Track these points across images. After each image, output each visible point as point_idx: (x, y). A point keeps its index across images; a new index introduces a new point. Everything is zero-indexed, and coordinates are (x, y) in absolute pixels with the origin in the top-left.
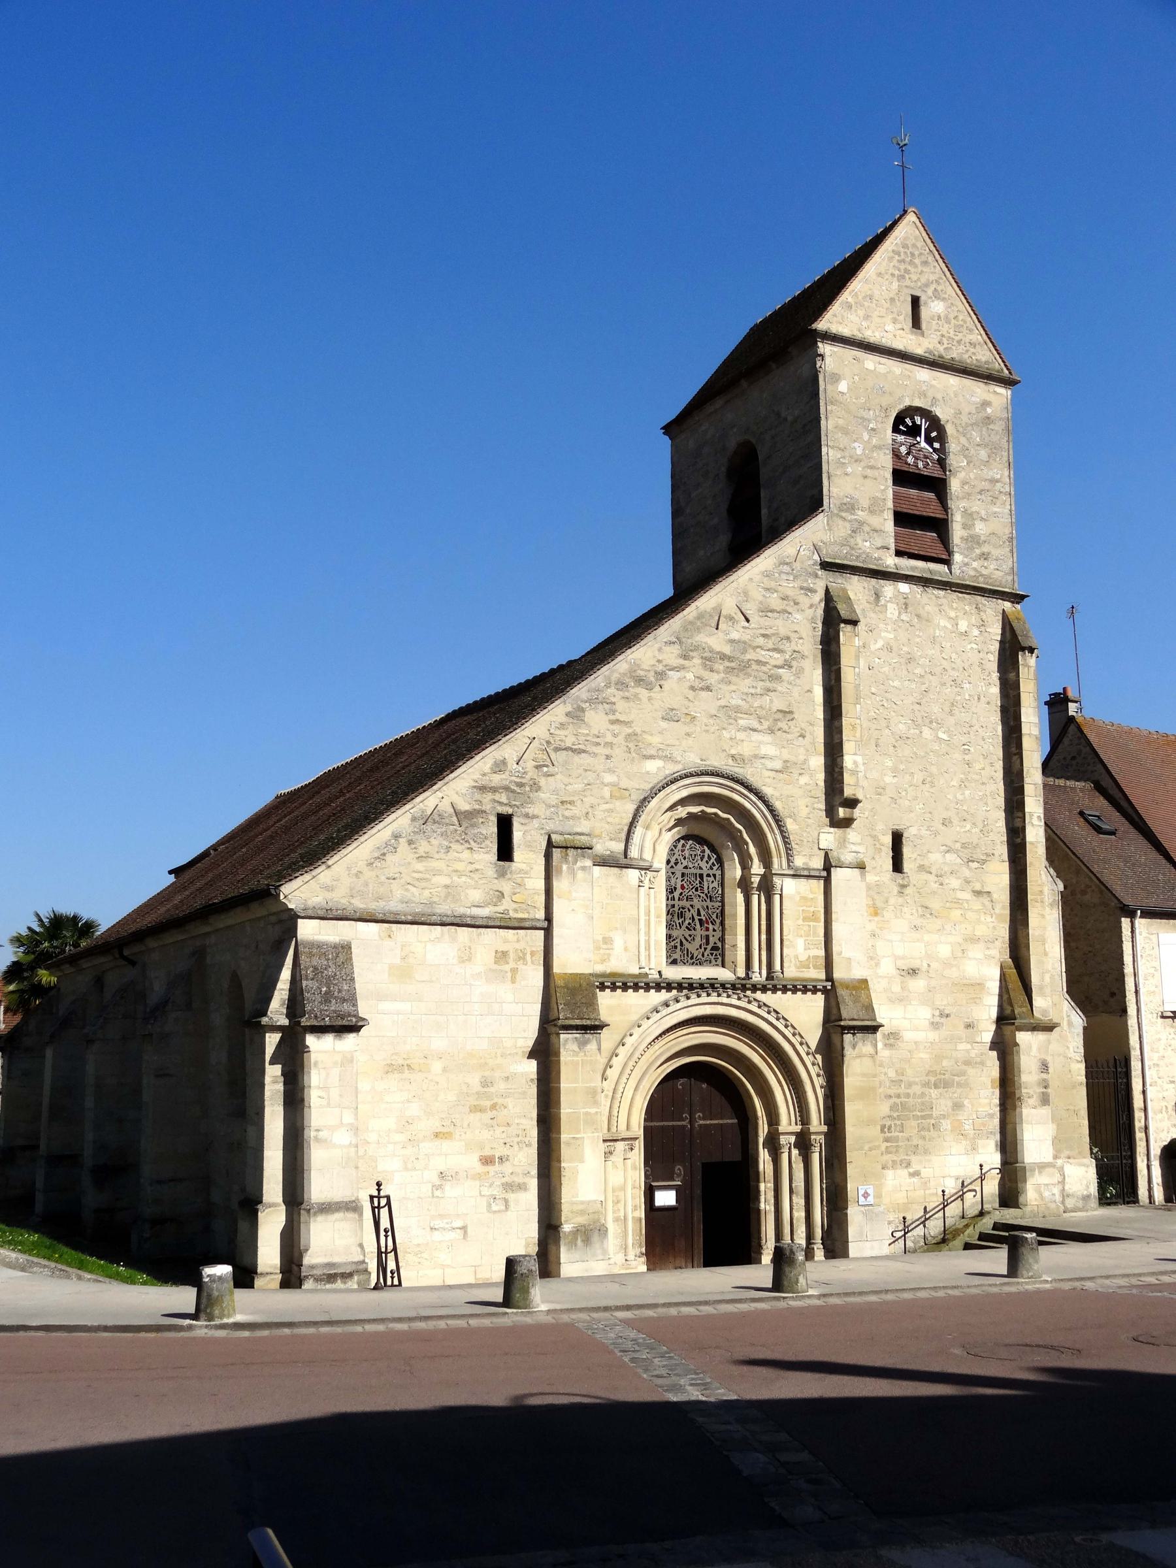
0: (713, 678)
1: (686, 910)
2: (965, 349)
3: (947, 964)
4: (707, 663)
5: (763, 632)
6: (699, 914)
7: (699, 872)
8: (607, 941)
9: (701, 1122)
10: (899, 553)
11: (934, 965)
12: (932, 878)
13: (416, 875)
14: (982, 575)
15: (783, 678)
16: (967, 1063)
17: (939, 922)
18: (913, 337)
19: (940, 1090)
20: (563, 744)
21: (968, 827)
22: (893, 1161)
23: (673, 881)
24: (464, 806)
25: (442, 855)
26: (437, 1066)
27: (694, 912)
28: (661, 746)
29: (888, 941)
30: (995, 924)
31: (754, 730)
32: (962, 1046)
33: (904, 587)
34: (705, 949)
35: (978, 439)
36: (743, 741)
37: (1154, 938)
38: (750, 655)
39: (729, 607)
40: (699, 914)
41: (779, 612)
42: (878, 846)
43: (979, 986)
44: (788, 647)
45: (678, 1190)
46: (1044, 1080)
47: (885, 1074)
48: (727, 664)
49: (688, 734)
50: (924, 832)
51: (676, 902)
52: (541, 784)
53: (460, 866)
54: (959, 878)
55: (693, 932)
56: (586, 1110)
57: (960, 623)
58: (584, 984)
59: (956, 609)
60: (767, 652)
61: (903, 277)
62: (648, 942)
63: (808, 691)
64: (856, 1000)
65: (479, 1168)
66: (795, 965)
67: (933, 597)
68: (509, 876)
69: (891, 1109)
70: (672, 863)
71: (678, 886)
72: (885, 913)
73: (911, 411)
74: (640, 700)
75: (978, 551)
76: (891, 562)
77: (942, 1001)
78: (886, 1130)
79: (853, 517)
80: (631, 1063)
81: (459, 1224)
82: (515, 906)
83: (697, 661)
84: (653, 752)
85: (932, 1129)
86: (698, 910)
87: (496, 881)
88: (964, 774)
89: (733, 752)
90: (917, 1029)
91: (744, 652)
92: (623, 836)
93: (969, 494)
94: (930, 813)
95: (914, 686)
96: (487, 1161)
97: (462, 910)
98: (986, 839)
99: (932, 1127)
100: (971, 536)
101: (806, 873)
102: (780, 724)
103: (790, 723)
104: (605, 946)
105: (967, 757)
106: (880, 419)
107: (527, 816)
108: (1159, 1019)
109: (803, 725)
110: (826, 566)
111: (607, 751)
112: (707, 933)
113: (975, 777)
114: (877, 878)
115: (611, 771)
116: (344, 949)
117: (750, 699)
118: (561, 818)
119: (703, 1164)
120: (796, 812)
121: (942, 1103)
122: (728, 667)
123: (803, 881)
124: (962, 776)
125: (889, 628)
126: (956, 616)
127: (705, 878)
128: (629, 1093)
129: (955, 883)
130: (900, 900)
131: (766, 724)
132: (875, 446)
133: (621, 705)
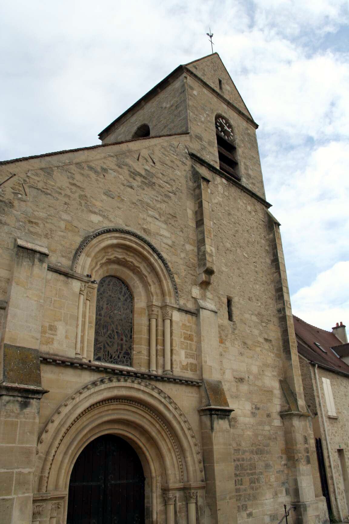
0: (135, 184)
1: (109, 324)
4: (132, 174)
8: (52, 328)
11: (251, 377)
19: (259, 456)
20: (35, 185)
21: (259, 304)
23: (101, 303)
28: (101, 209)
31: (157, 219)
34: (120, 353)
36: (150, 223)
39: (145, 153)
43: (270, 392)
51: (102, 317)
52: (14, 204)
55: (112, 340)
56: (19, 470)
62: (82, 337)
63: (185, 210)
66: (180, 367)
71: (105, 306)
74: (91, 178)
80: (64, 430)
84: (97, 211)
86: (117, 325)
89: (145, 226)
90: (245, 416)
92: (71, 256)
94: (243, 292)
104: (50, 332)
111: (67, 200)
117: (154, 201)
118: (26, 231)
121: (260, 465)
122: (143, 181)
128: (59, 457)
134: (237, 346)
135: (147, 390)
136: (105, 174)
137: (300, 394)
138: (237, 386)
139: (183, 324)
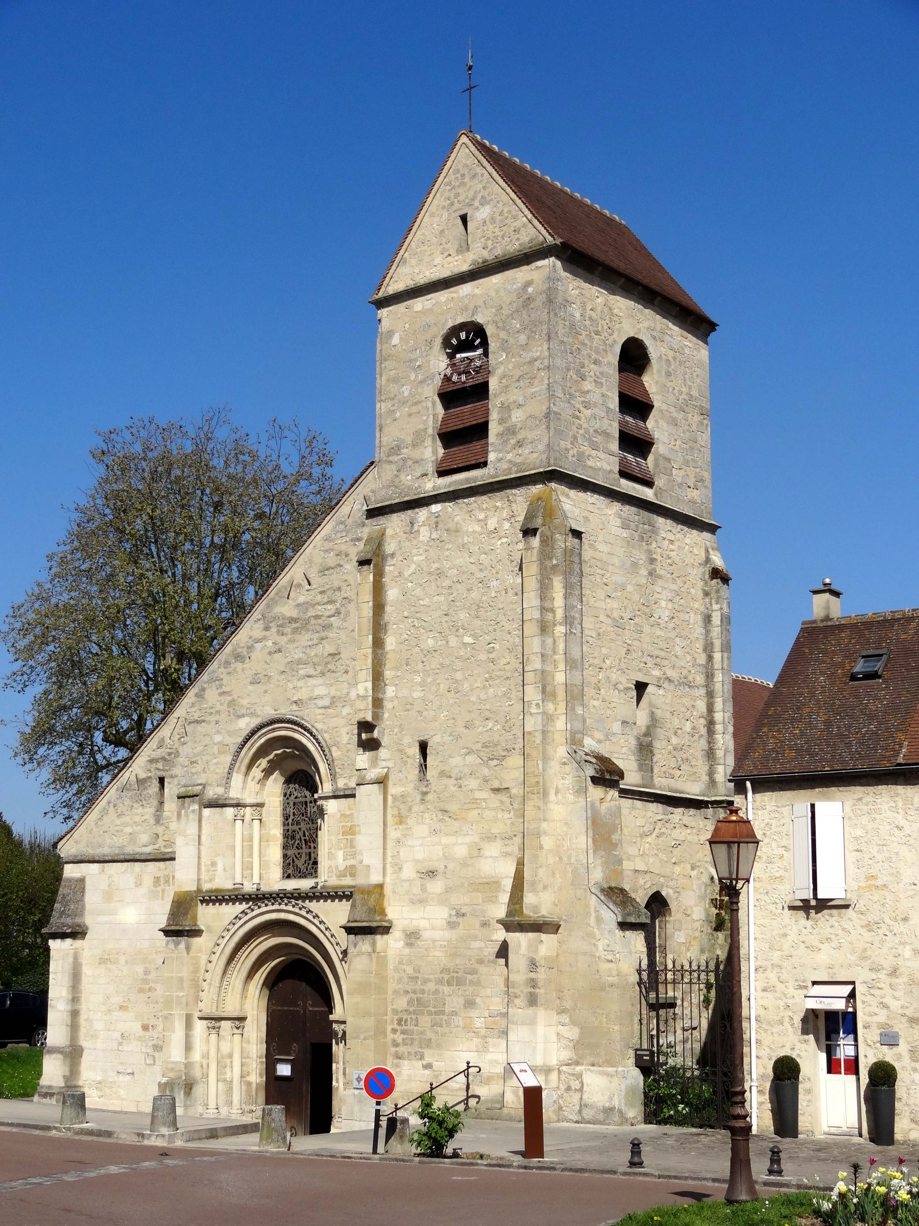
2: (509, 240)
3: (464, 864)
5: (320, 590)
6: (304, 836)
7: (304, 800)
8: (214, 864)
9: (311, 1009)
10: (442, 473)
11: (451, 866)
12: (452, 782)
13: (117, 828)
14: (515, 464)
15: (334, 625)
16: (480, 961)
17: (456, 825)
18: (460, 257)
19: (452, 988)
22: (409, 1052)
23: (288, 809)
24: (142, 775)
25: (129, 812)
26: (122, 959)
27: (301, 834)
29: (410, 846)
30: (513, 820)
32: (476, 944)
33: (436, 508)
34: (309, 864)
35: (518, 326)
36: (301, 688)
38: (311, 613)
39: (299, 578)
40: (304, 836)
41: (333, 568)
46: (533, 980)
47: (405, 971)
48: (294, 625)
49: (266, 692)
50: (447, 738)
54: (478, 778)
55: (300, 851)
57: (489, 522)
58: (188, 898)
59: (487, 509)
60: (323, 607)
61: (452, 204)
64: (365, 902)
65: (141, 1032)
67: (464, 506)
68: (161, 822)
69: (410, 1003)
70: (288, 796)
72: (409, 821)
73: (455, 331)
74: (237, 672)
75: (513, 442)
76: (433, 484)
77: (460, 899)
78: (403, 1023)
79: (399, 457)
81: (130, 1071)
82: (165, 843)
83: (274, 630)
84: (243, 711)
85: (444, 1025)
87: (154, 827)
88: (488, 673)
89: (295, 699)
90: (434, 928)
91: (307, 610)
93: (507, 387)
95: (442, 598)
96: (145, 1028)
97: (138, 850)
98: (508, 734)
99: (444, 1023)
100: (508, 429)
101: (342, 793)
102: (329, 666)
103: (336, 663)
105: (491, 656)
106: (424, 354)
107: (172, 777)
109: (347, 662)
110: (373, 513)
112: (310, 850)
114: (403, 789)
115: (218, 732)
116: (82, 881)
117: (308, 651)
119: (312, 1044)
120: (338, 739)
121: (454, 1002)
124: (487, 676)
125: (421, 551)
127: (308, 804)
129: (473, 783)
130: (422, 807)
131: (319, 668)
132: (420, 382)
133: (226, 679)
134: (427, 821)
135: (296, 910)
136: (250, 655)
138: (422, 885)
139: (342, 815)
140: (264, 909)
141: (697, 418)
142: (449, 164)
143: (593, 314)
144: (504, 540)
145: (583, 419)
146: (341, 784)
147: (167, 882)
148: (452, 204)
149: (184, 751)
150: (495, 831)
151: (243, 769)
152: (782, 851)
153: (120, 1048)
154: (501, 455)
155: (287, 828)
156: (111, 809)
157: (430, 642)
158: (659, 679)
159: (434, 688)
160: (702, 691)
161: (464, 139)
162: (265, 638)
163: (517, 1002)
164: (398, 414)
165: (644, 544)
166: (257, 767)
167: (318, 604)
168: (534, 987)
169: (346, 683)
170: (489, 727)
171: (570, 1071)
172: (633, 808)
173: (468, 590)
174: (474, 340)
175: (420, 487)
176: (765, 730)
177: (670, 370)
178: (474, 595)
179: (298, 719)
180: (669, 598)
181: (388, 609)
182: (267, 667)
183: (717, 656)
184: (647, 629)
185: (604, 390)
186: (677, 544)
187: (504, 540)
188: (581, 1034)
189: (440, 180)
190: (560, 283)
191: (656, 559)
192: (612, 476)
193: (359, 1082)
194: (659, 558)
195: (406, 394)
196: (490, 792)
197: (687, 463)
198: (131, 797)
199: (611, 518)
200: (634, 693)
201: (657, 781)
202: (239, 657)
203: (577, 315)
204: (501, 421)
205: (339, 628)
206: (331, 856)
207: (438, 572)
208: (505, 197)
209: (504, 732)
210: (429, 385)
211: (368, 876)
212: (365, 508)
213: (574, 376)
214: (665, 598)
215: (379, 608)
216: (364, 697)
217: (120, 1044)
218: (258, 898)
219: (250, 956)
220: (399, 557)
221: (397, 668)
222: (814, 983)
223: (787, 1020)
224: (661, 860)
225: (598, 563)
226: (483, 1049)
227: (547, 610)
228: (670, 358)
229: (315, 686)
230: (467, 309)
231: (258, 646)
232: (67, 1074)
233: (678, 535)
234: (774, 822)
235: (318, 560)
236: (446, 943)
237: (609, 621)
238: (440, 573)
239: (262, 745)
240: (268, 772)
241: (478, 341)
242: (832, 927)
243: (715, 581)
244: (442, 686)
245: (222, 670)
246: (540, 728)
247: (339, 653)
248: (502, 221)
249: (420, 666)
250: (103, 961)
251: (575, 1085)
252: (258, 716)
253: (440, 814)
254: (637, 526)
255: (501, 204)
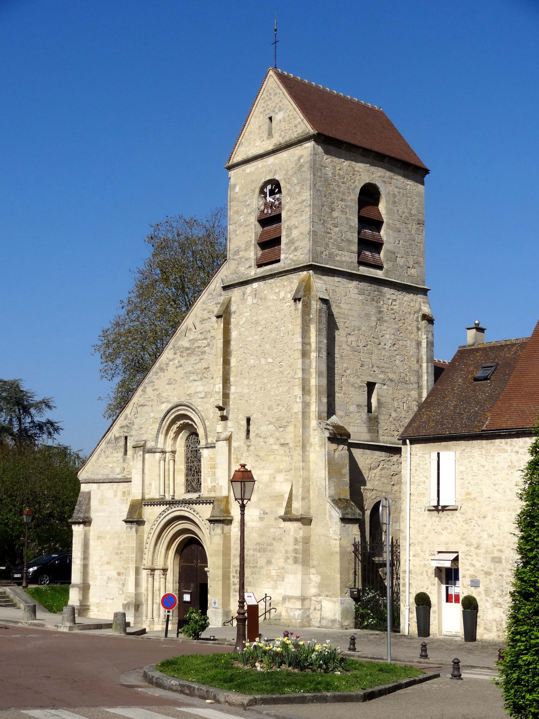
3: (267, 486)
5: (201, 332)
6: (196, 469)
10: (259, 266)
12: (262, 440)
13: (105, 464)
14: (293, 261)
15: (207, 352)
16: (274, 539)
18: (268, 141)
19: (261, 553)
23: (188, 454)
24: (117, 435)
26: (108, 537)
32: (272, 530)
33: (255, 285)
35: (296, 181)
36: (191, 387)
37: (427, 456)
38: (196, 345)
40: (196, 469)
42: (240, 427)
44: (209, 335)
45: (191, 594)
46: (296, 549)
48: (188, 352)
49: (174, 389)
50: (260, 416)
53: (115, 459)
58: (137, 503)
60: (201, 341)
61: (265, 111)
65: (116, 576)
68: (126, 461)
75: (293, 248)
76: (254, 272)
79: (239, 257)
81: (112, 597)
82: (127, 473)
83: (178, 354)
84: (164, 400)
85: (257, 574)
87: (123, 464)
89: (188, 393)
93: (290, 217)
96: (119, 574)
100: (290, 241)
101: (209, 446)
102: (205, 375)
105: (281, 369)
107: (131, 436)
108: (427, 512)
110: (225, 288)
113: (285, 379)
114: (238, 444)
115: (152, 411)
116: (89, 493)
119: (200, 584)
121: (262, 562)
123: (210, 449)
125: (248, 310)
126: (279, 291)
129: (271, 441)
130: (247, 454)
131: (200, 376)
137: (297, 496)
139: (210, 458)
140: (174, 509)
141: (415, 227)
142: (263, 87)
143: (341, 172)
144: (288, 304)
145: (333, 234)
146: (210, 440)
147: (129, 494)
148: (265, 111)
149: (137, 421)
150: (281, 467)
151: (164, 432)
152: (425, 479)
153: (107, 585)
154: (287, 256)
155: (188, 464)
156: (103, 454)
157: (252, 361)
158: (384, 380)
159: (254, 388)
160: (415, 386)
161: (271, 73)
162: (174, 359)
163: (289, 561)
164: (238, 232)
165: (374, 302)
166: (172, 431)
167: (199, 340)
168: (296, 553)
169: (212, 384)
170: (280, 409)
171: (316, 599)
172: (364, 454)
173: (270, 332)
174: (275, 190)
175: (248, 274)
176: (423, 410)
177: (396, 199)
178: (273, 335)
179: (188, 404)
180: (392, 333)
181: (232, 343)
182: (175, 375)
183: (424, 365)
184: (376, 351)
185: (348, 216)
186: (398, 301)
187: (288, 304)
188: (322, 579)
189: (259, 96)
190: (317, 156)
191: (383, 311)
192: (353, 265)
193: (215, 604)
194: (385, 310)
195: (242, 220)
196: (280, 445)
197: (407, 254)
198: (112, 448)
199: (351, 289)
200: (366, 389)
201: (381, 438)
202: (162, 369)
203: (330, 174)
204: (287, 236)
205: (209, 353)
206: (206, 481)
207: (256, 322)
208: (291, 107)
209: (286, 412)
210: (253, 215)
211: (221, 491)
212: (222, 285)
213: (327, 209)
214: (389, 333)
215: (227, 342)
216: (219, 393)
217: (107, 583)
218: (173, 503)
219: (168, 535)
220: (237, 314)
221: (236, 376)
222: (439, 552)
223: (425, 572)
224: (383, 483)
225: (342, 316)
226: (275, 587)
227: (306, 344)
228: (396, 193)
229: (198, 386)
230: (271, 171)
231: (171, 363)
232: (81, 599)
233: (399, 296)
234: (421, 462)
235: (200, 315)
236: (258, 529)
237: (349, 348)
238: (257, 323)
239: (173, 419)
240: (177, 433)
241: (277, 190)
242: (448, 521)
243: (424, 321)
244: (257, 386)
245: (154, 376)
246: (301, 410)
247: (209, 368)
248: (289, 121)
249: (247, 375)
250: (99, 537)
251: (318, 607)
252: (171, 402)
253: (256, 457)
254: (370, 293)
255: (288, 110)
